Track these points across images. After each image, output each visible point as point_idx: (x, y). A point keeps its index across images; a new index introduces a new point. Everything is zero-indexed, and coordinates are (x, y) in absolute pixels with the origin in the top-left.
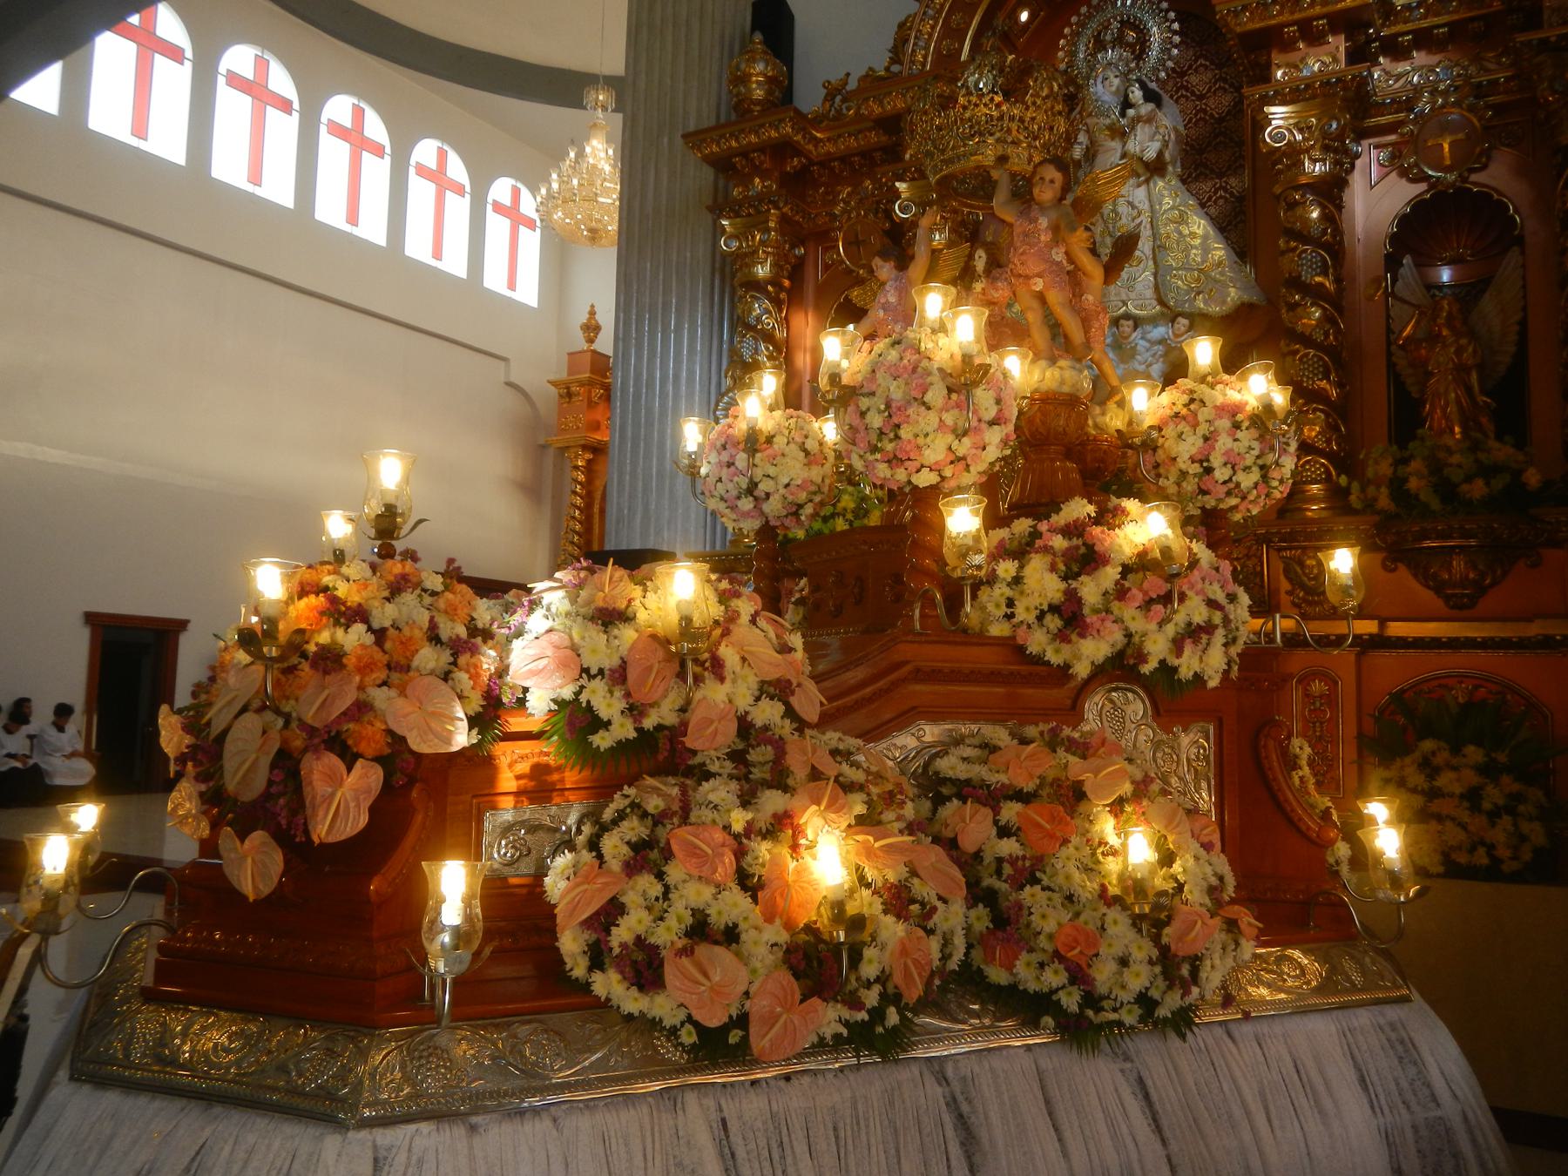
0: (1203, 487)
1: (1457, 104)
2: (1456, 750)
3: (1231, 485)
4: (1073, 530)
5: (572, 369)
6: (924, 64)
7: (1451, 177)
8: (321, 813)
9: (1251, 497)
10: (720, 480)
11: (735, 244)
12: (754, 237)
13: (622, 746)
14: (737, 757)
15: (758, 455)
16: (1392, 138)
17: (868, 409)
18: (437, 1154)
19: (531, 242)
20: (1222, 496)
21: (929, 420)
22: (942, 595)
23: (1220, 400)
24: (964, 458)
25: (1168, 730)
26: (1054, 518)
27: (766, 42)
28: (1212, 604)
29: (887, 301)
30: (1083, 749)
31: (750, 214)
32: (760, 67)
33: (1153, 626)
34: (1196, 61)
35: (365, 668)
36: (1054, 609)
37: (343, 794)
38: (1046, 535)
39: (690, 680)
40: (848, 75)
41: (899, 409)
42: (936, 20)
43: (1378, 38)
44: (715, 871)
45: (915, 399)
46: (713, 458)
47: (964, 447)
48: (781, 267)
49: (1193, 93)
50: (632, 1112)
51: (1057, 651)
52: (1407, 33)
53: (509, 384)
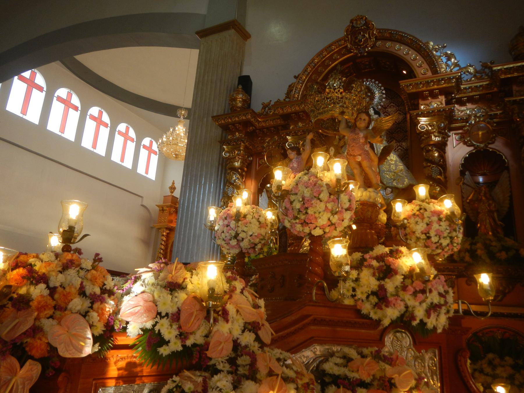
0: (427, 244)
1: (484, 121)
2: (502, 357)
3: (438, 244)
4: (380, 258)
5: (164, 202)
6: (298, 98)
7: (482, 145)
9: (446, 250)
10: (223, 232)
11: (228, 155)
12: (235, 152)
13: (174, 354)
14: (232, 361)
15: (240, 222)
16: (460, 131)
17: (294, 200)
19: (155, 159)
21: (321, 206)
22: (327, 284)
23: (433, 209)
24: (334, 224)
25: (420, 352)
26: (371, 253)
27: (243, 88)
28: (440, 295)
29: (293, 166)
30: (390, 360)
31: (234, 145)
32: (241, 96)
33: (417, 304)
34: (390, 104)
35: (41, 308)
36: (373, 293)
37: (16, 380)
38: (369, 260)
39: (212, 321)
40: (271, 101)
41: (308, 201)
42: (302, 84)
43: (455, 98)
45: (315, 197)
46: (221, 223)
47: (335, 219)
48: (244, 164)
51: (375, 313)
52: (465, 97)
53: (142, 205)
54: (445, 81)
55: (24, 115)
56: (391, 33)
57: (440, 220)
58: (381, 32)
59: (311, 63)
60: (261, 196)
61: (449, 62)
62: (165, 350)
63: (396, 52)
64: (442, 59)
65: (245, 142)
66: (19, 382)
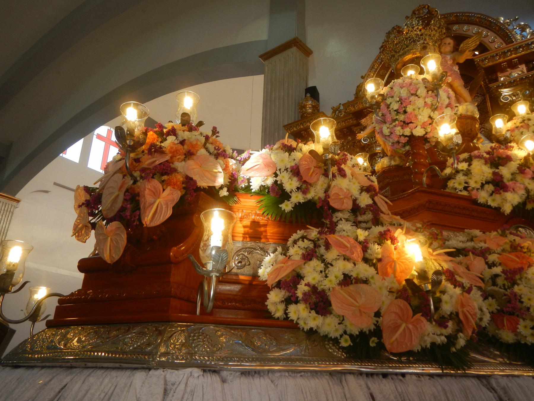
8: (148, 212)
17: (391, 103)
18: (203, 389)
21: (420, 102)
22: (439, 168)
32: (310, 102)
39: (331, 176)
44: (353, 253)
45: (412, 94)
50: (317, 381)
51: (494, 200)
54: (523, 48)
56: (457, 16)
58: (446, 17)
59: (377, 60)
61: (524, 33)
62: (287, 206)
63: (465, 33)
64: (515, 32)
66: (162, 203)
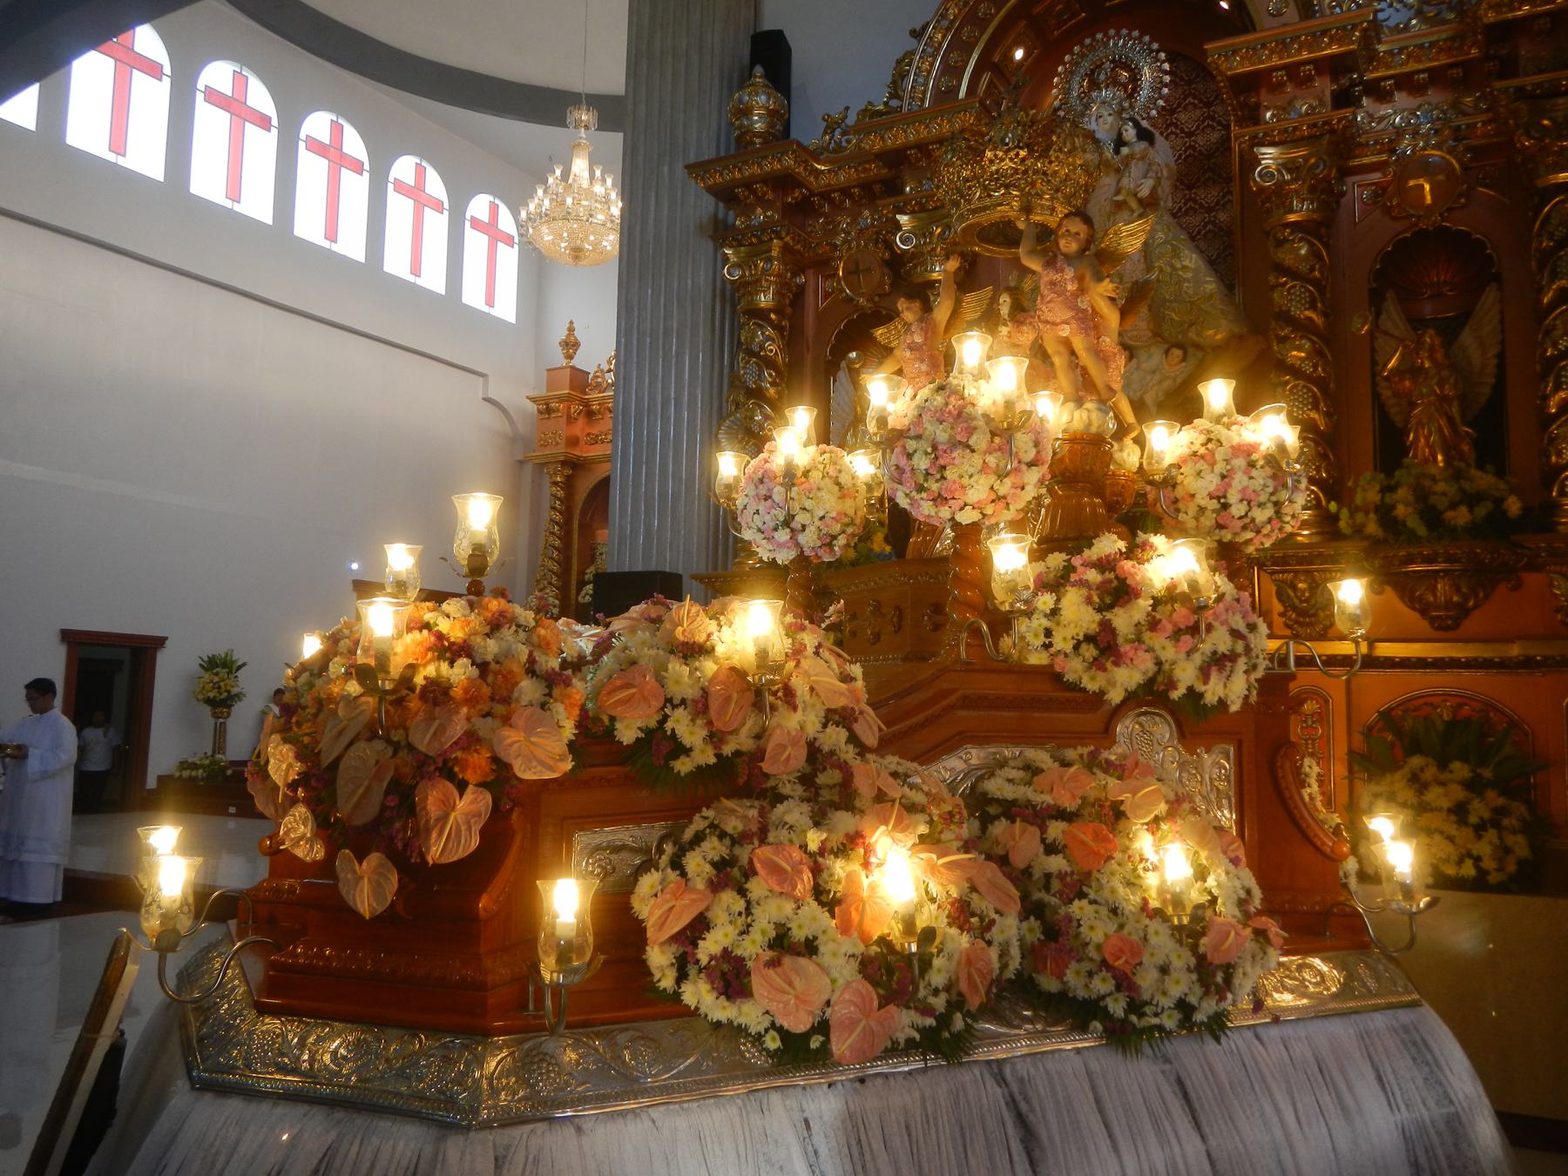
0: (1221, 522)
2: (1443, 765)
3: (1247, 521)
4: (1104, 565)
6: (923, 100)
8: (434, 835)
9: (1265, 531)
10: (757, 512)
11: (737, 274)
12: (756, 266)
13: (701, 771)
14: (806, 780)
15: (795, 489)
16: (1376, 177)
17: (915, 451)
19: (509, 258)
20: (1238, 530)
23: (1236, 440)
24: (1004, 497)
25: (1192, 752)
26: (1087, 553)
27: (767, 76)
28: (1235, 634)
29: (913, 342)
30: (1119, 770)
31: (755, 246)
33: (1183, 655)
34: (1185, 99)
35: (471, 700)
36: (1089, 639)
37: (455, 818)
38: (1080, 569)
40: (847, 108)
41: (945, 452)
43: (1361, 82)
44: (794, 888)
46: (751, 490)
47: (1004, 488)
49: (1182, 131)
51: (1093, 678)
55: (118, 154)
57: (1252, 465)
60: (835, 381)
65: (783, 234)
